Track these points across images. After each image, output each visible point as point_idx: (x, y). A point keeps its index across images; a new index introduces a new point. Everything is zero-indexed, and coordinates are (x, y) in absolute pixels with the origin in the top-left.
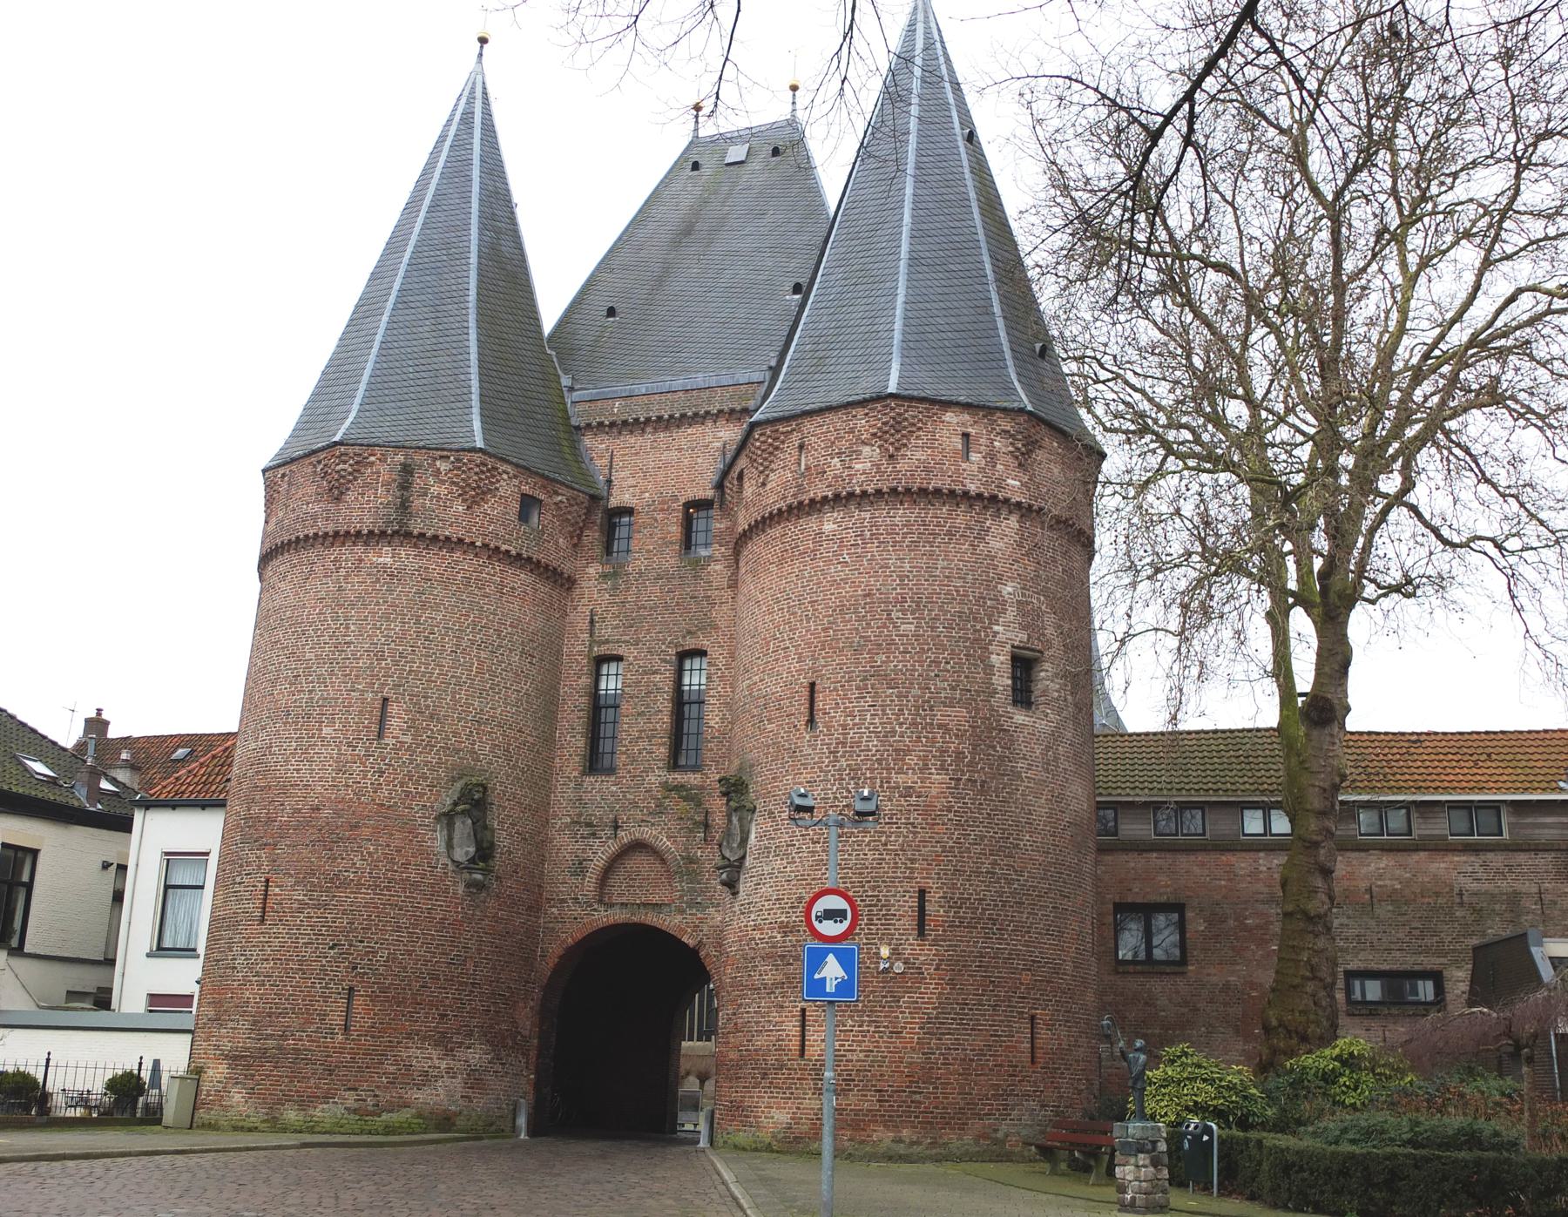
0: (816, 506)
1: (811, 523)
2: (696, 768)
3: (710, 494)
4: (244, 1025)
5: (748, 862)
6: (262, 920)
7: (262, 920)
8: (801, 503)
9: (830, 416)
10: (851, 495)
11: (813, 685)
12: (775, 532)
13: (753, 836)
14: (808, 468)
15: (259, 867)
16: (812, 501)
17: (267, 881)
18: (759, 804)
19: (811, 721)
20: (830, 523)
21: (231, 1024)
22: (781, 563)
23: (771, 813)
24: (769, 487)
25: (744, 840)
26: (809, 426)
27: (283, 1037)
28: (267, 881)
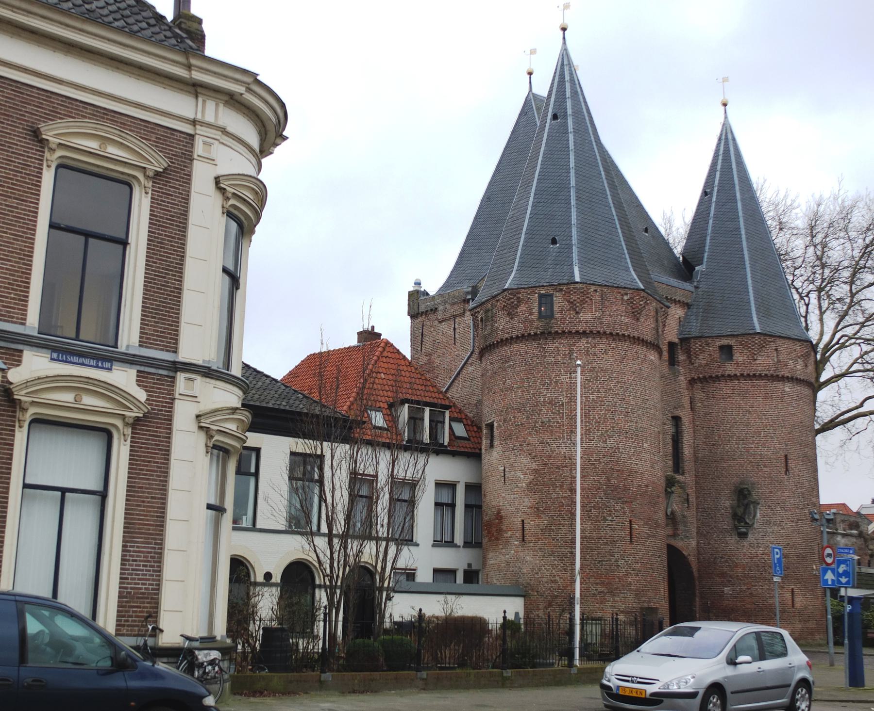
0: (783, 379)
1: (780, 385)
2: (683, 474)
3: (677, 341)
4: (631, 597)
5: (755, 526)
6: (631, 541)
7: (631, 541)
8: (778, 376)
9: (787, 342)
10: (797, 379)
11: (786, 456)
12: (762, 383)
13: (758, 514)
14: (779, 361)
15: (624, 513)
16: (783, 377)
17: (630, 521)
18: (762, 502)
19: (787, 470)
20: (788, 388)
21: (622, 595)
22: (765, 398)
23: (769, 506)
24: (758, 362)
25: (755, 516)
26: (779, 342)
27: (649, 602)
28: (630, 521)
